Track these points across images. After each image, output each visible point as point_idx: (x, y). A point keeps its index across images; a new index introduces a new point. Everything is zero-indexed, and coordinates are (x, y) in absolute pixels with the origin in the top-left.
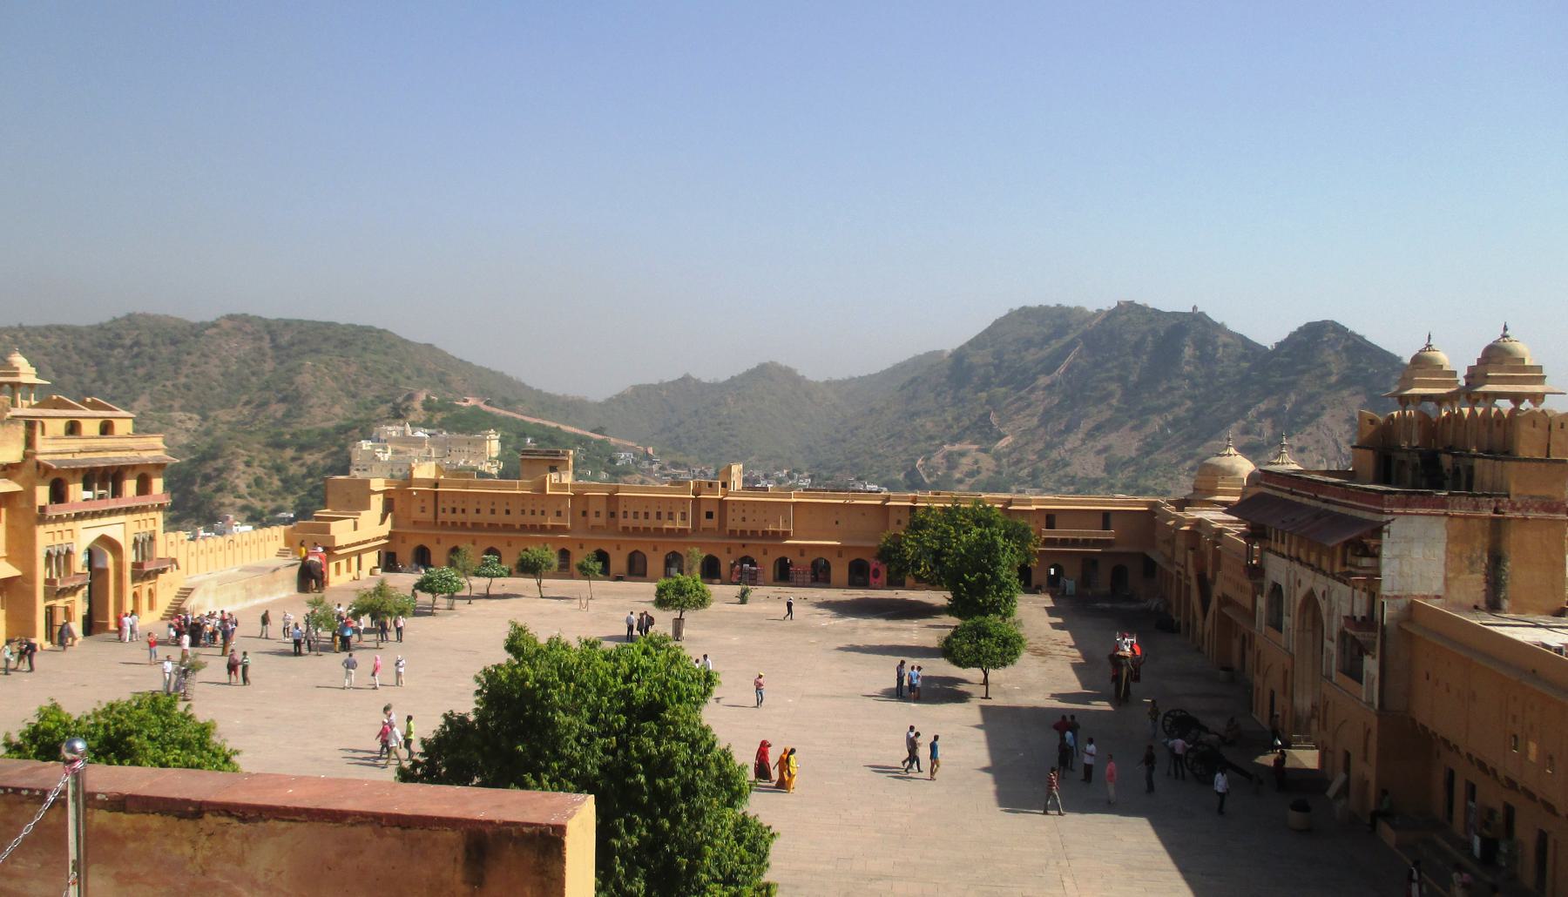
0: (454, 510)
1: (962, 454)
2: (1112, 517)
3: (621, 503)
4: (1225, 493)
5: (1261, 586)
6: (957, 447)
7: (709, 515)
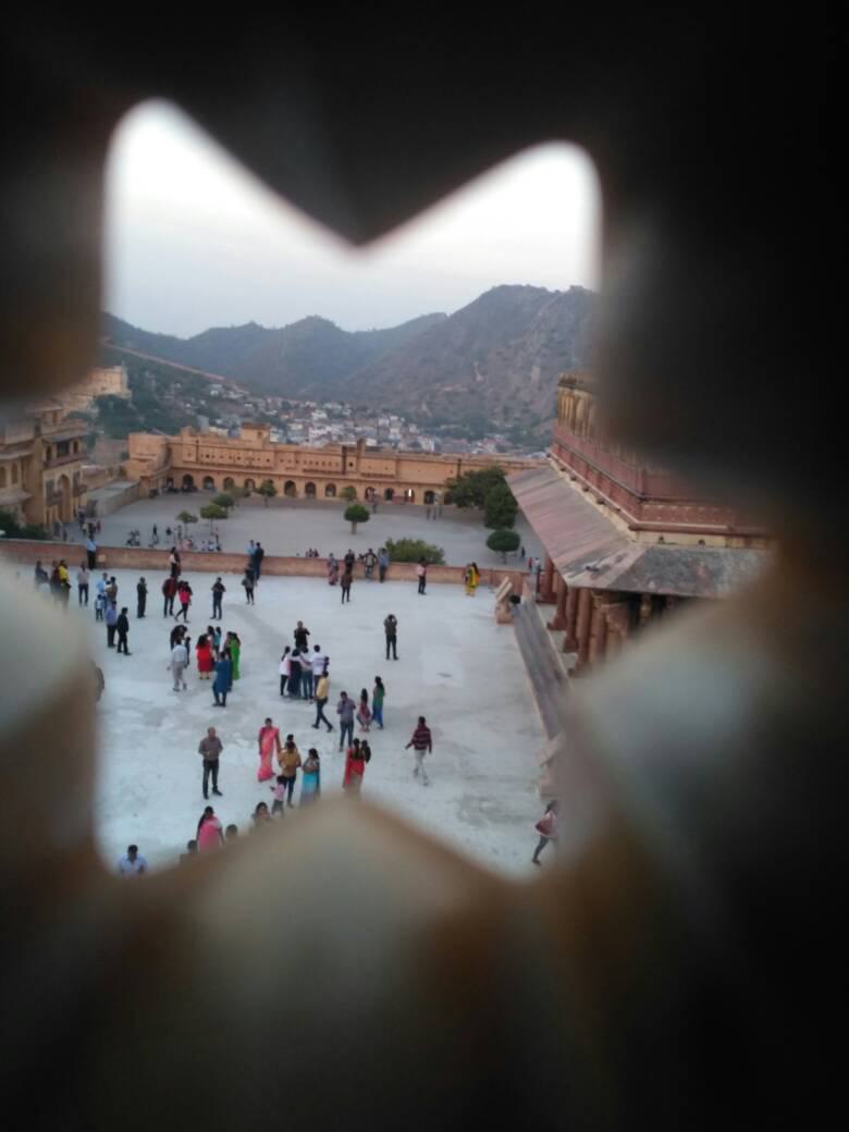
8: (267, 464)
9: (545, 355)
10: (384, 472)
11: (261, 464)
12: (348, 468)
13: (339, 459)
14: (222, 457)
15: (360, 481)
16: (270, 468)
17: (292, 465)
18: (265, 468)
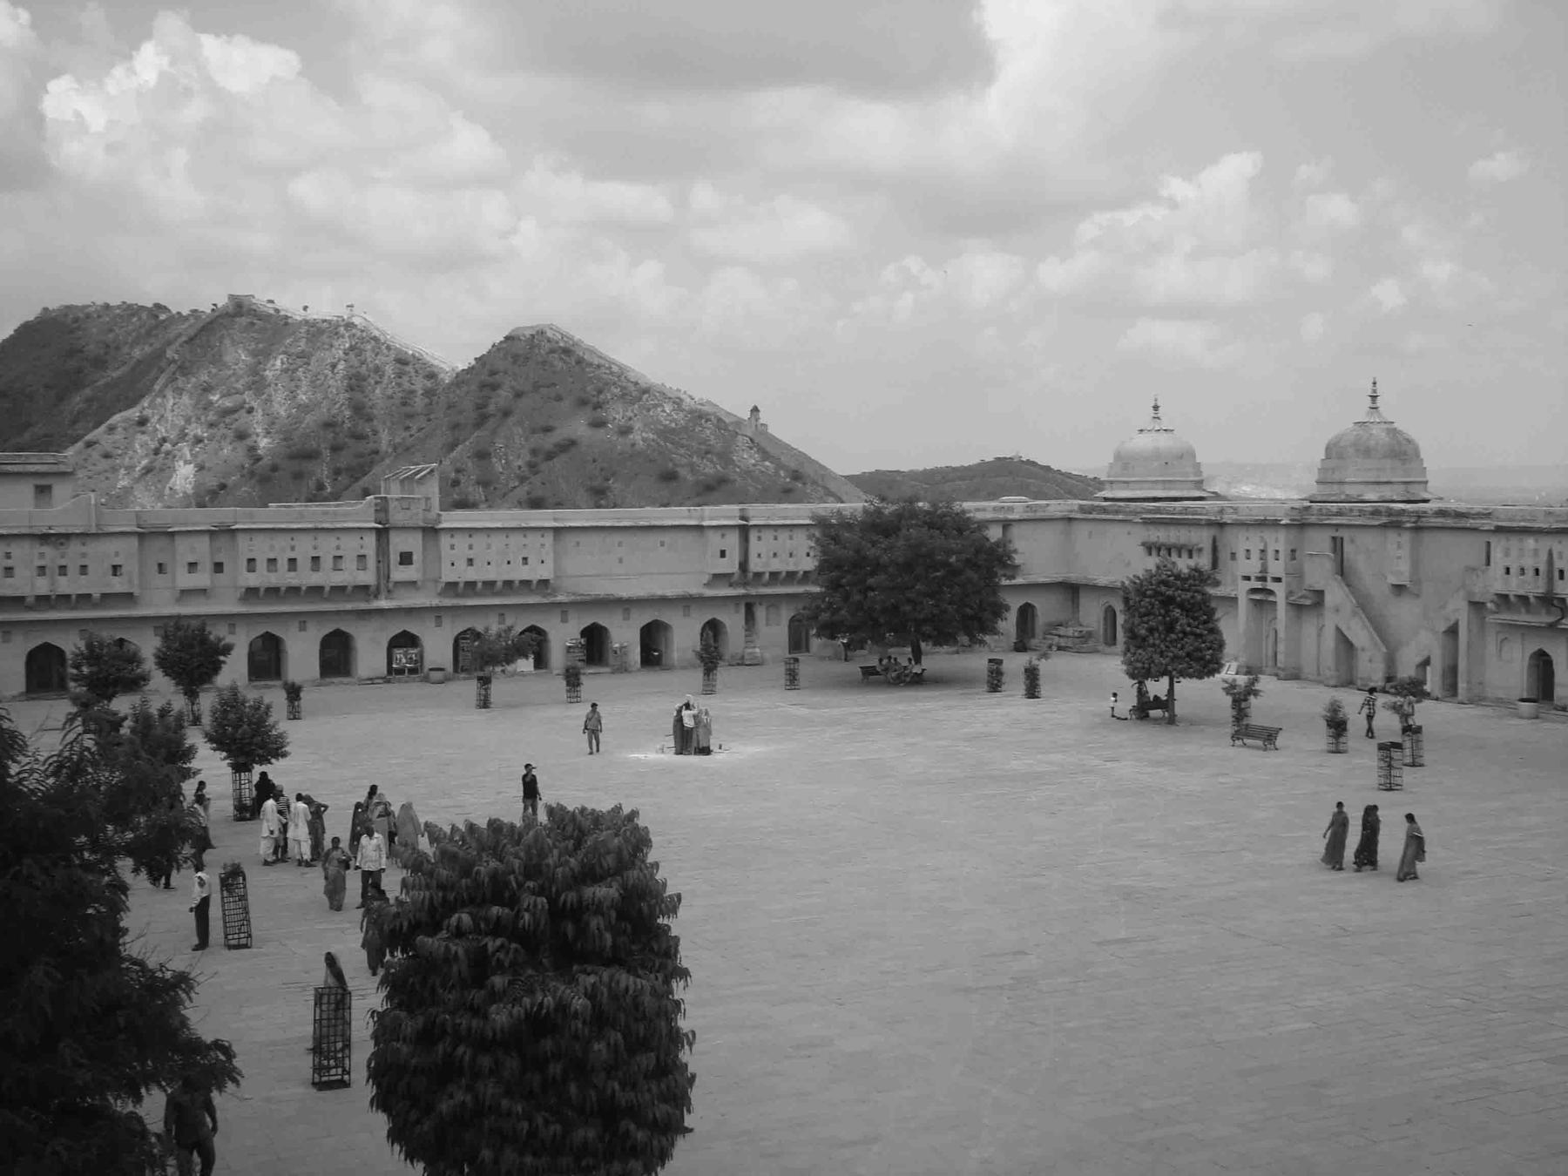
7: (406, 559)
8: (118, 585)
9: (199, 440)
10: (520, 573)
11: (94, 584)
13: (370, 541)
15: (437, 613)
16: (128, 598)
17: (202, 579)
18: (108, 598)
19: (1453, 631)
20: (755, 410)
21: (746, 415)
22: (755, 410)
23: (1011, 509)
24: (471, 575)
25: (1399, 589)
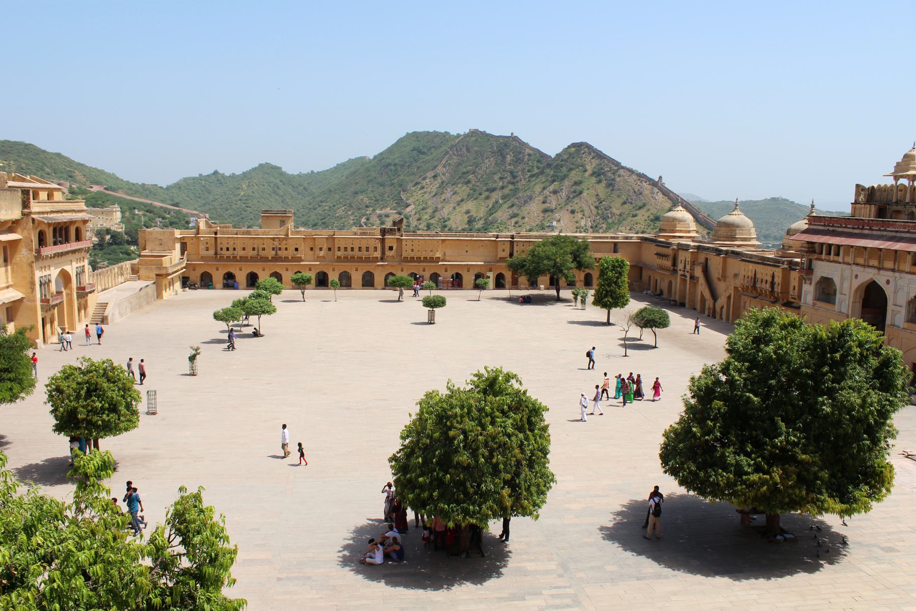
0: (228, 249)
1: (387, 216)
2: (619, 246)
3: (336, 241)
4: (680, 231)
5: (810, 279)
6: (383, 212)
7: (391, 248)
12: (388, 253)
14: (244, 249)
19: (729, 297)
20: (660, 177)
21: (657, 180)
22: (660, 177)
23: (617, 238)
24: (412, 254)
25: (719, 279)
